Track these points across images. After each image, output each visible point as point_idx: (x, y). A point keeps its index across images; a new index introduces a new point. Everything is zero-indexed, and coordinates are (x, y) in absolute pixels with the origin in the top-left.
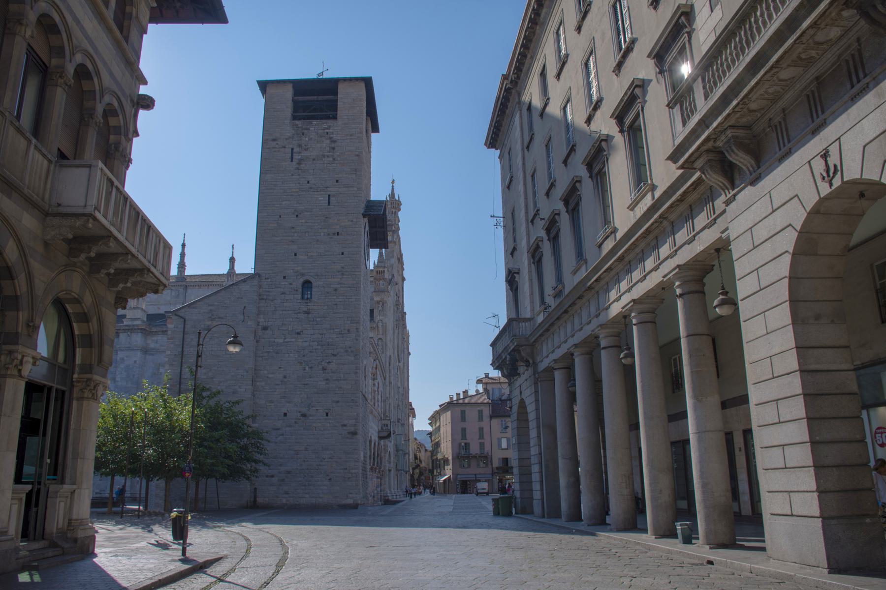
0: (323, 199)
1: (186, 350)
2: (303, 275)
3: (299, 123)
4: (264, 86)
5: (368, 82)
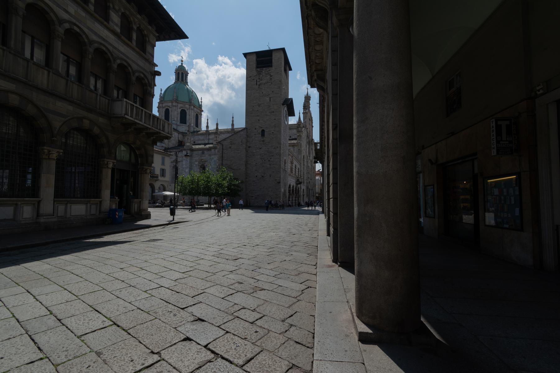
0: (268, 99)
3: (258, 69)
4: (245, 55)
5: (283, 50)
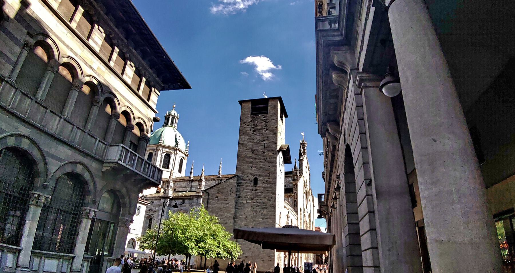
0: (262, 145)
1: (209, 206)
2: (254, 175)
4: (241, 102)
